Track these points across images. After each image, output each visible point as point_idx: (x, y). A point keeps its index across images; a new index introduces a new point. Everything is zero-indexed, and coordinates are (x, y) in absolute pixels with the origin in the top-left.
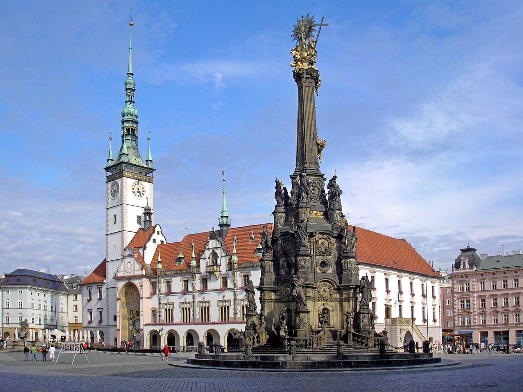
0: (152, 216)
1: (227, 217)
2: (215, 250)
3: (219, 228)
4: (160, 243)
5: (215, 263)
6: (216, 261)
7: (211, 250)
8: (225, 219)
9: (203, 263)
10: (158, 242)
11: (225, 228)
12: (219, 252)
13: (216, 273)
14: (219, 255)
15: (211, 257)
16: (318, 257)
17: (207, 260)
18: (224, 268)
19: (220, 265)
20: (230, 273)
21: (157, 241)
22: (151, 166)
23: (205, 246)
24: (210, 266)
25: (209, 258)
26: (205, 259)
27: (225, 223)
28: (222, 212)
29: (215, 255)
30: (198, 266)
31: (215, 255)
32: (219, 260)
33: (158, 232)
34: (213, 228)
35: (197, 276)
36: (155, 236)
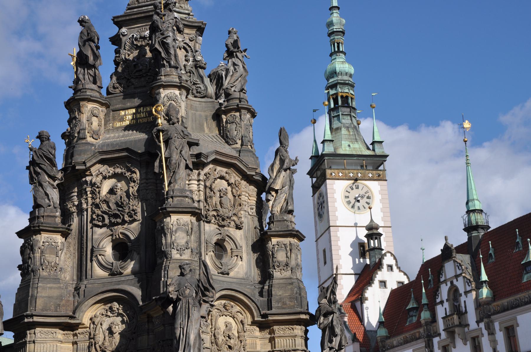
0: (382, 238)
1: (481, 211)
2: (455, 281)
3: (464, 238)
4: (395, 286)
5: (458, 311)
6: (459, 305)
7: (449, 284)
8: (473, 216)
9: (441, 311)
10: (392, 285)
11: (475, 234)
12: (460, 284)
13: (457, 330)
14: (462, 290)
15: (452, 297)
16: (99, 231)
17: (446, 305)
18: (472, 317)
19: (466, 312)
20: (482, 325)
21: (388, 284)
22: (378, 151)
23: (439, 278)
24: (450, 316)
25: (447, 300)
26: (442, 302)
27: (474, 223)
28: (467, 203)
29: (454, 293)
30: (434, 319)
31: (454, 293)
32: (463, 299)
33: (390, 267)
34: (446, 238)
35: (436, 340)
36: (380, 276)
